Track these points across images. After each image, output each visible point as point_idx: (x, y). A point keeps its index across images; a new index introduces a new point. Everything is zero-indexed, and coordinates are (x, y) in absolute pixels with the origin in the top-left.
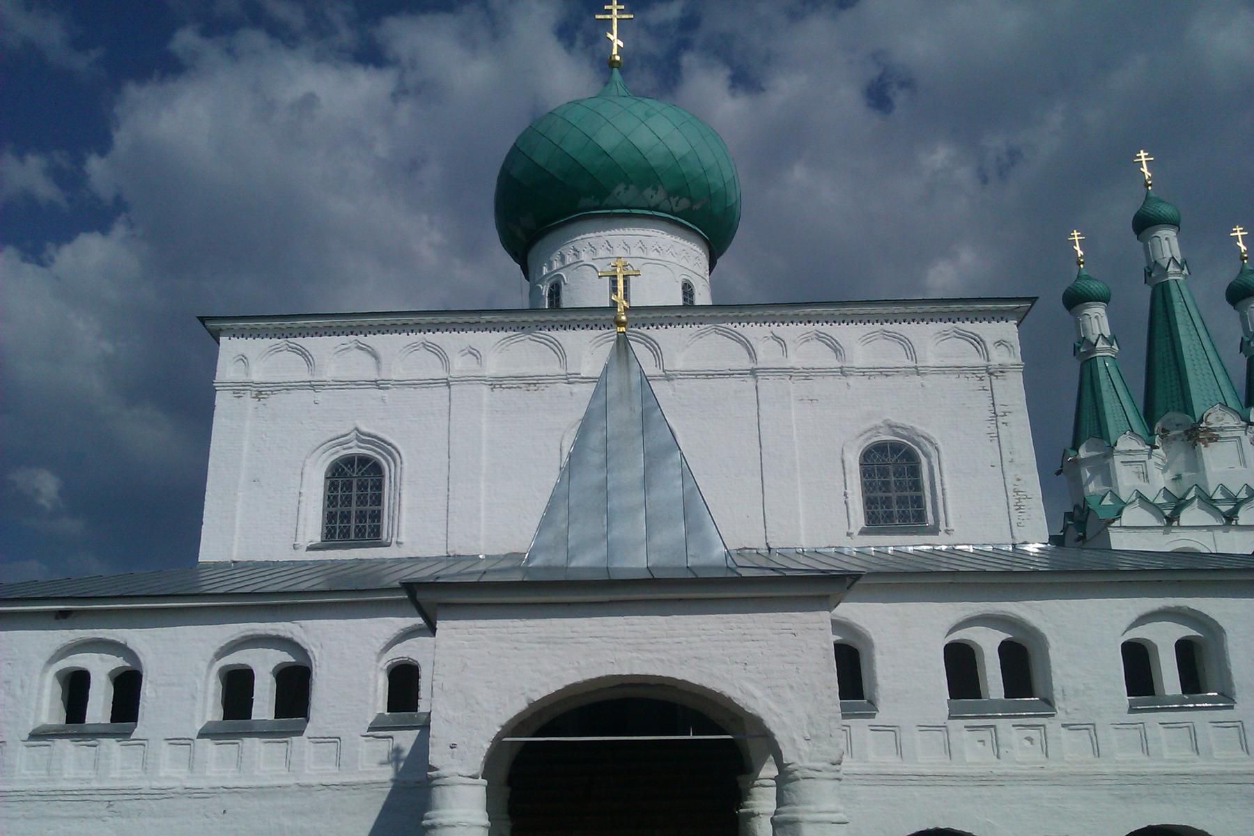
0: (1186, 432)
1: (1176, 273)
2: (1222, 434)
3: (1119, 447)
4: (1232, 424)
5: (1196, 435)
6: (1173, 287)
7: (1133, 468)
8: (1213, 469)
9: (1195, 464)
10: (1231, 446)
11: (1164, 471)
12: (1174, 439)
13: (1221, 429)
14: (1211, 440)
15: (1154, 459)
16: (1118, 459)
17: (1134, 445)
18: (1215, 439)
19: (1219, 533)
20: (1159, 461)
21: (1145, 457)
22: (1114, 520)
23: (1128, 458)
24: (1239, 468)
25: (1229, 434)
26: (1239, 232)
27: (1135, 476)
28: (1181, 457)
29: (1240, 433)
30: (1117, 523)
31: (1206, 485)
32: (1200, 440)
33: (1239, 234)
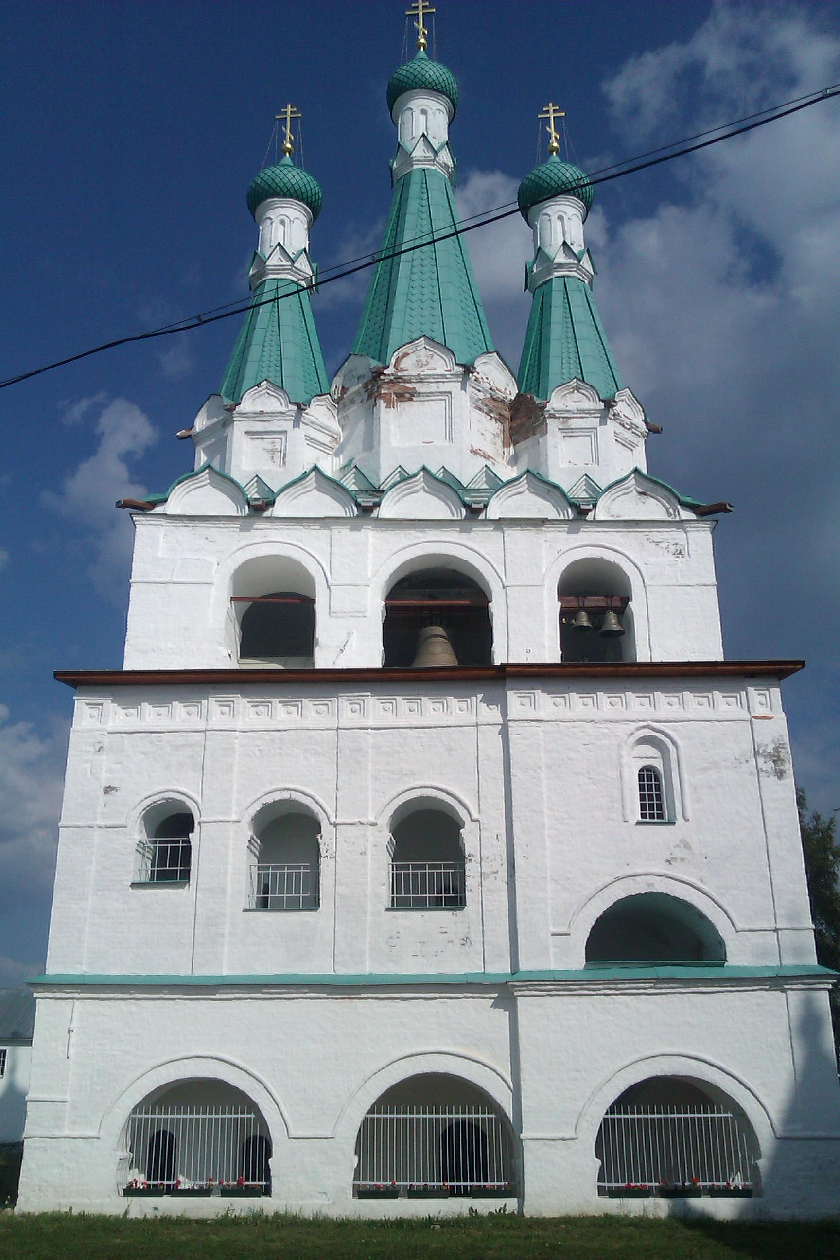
0: (366, 386)
1: (426, 160)
2: (420, 388)
3: (248, 404)
4: (440, 371)
5: (377, 388)
6: (416, 180)
7: (266, 444)
8: (394, 443)
9: (371, 442)
10: (437, 407)
11: (337, 454)
12: (352, 401)
13: (421, 380)
14: (401, 397)
15: (303, 430)
16: (239, 428)
17: (273, 404)
18: (406, 396)
19: (342, 534)
20: (326, 440)
21: (288, 425)
22: (153, 504)
23: (258, 427)
24: (440, 442)
25: (433, 388)
26: (552, 112)
27: (267, 456)
28: (361, 428)
29: (455, 387)
30: (158, 510)
31: (377, 472)
32: (380, 395)
33: (552, 116)
